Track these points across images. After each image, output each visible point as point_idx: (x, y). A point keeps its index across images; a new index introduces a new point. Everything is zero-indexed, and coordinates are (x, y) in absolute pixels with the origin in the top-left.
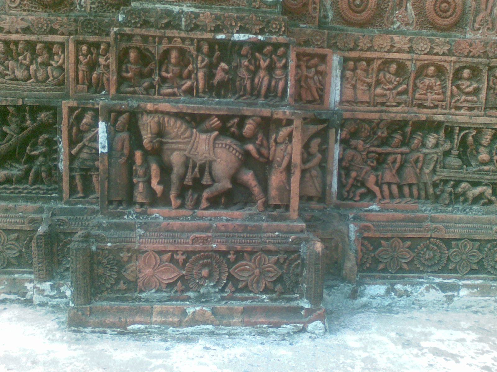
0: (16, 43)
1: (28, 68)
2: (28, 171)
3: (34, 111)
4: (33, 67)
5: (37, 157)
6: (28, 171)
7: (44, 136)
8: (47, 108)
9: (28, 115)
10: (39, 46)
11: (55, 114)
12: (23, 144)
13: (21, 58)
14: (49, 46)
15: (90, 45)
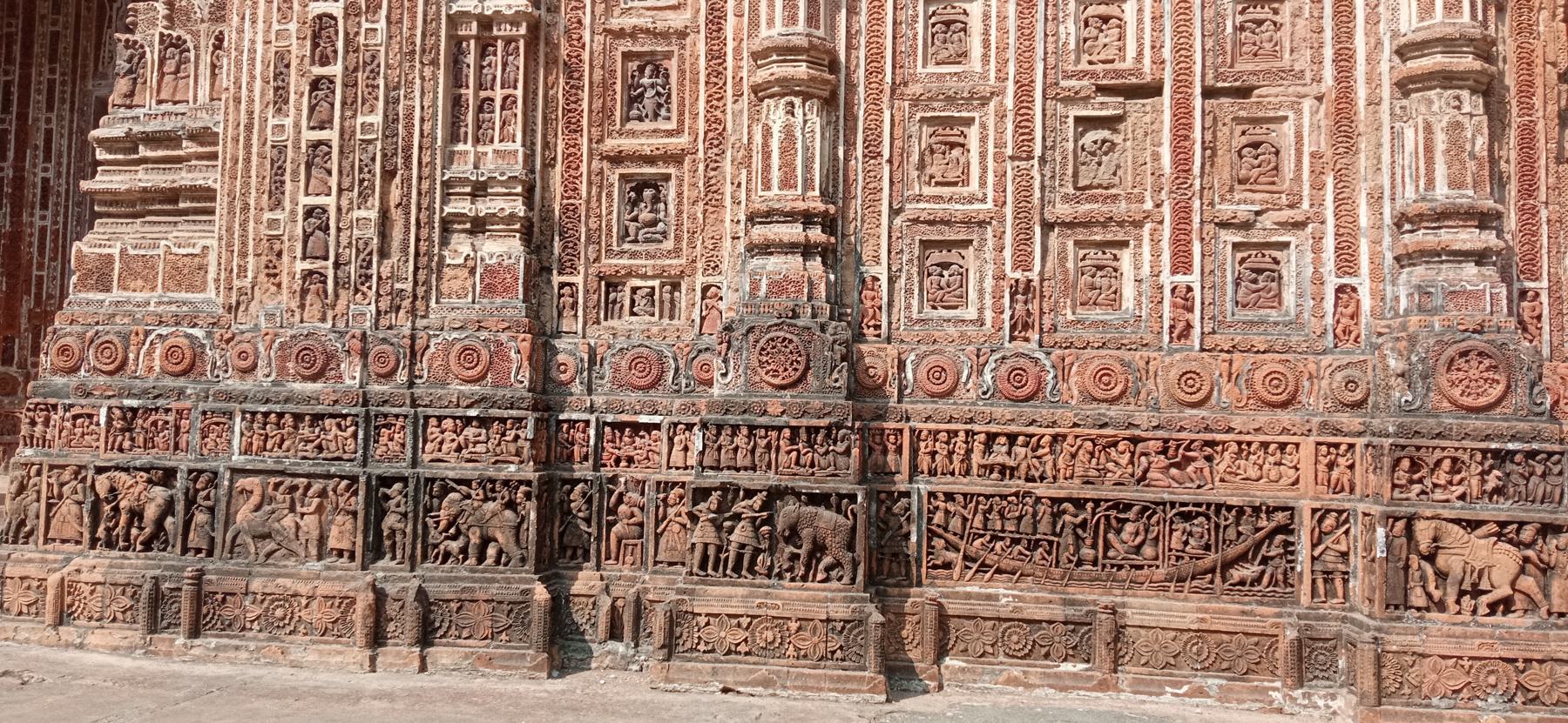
0: (1249, 444)
1: (1261, 468)
2: (1263, 572)
3: (1271, 511)
4: (1266, 466)
5: (1272, 558)
6: (1263, 572)
7: (1279, 538)
8: (1284, 509)
9: (1263, 515)
10: (1273, 447)
11: (1292, 516)
12: (1258, 546)
13: (1253, 458)
14: (1282, 446)
15: (1329, 445)
